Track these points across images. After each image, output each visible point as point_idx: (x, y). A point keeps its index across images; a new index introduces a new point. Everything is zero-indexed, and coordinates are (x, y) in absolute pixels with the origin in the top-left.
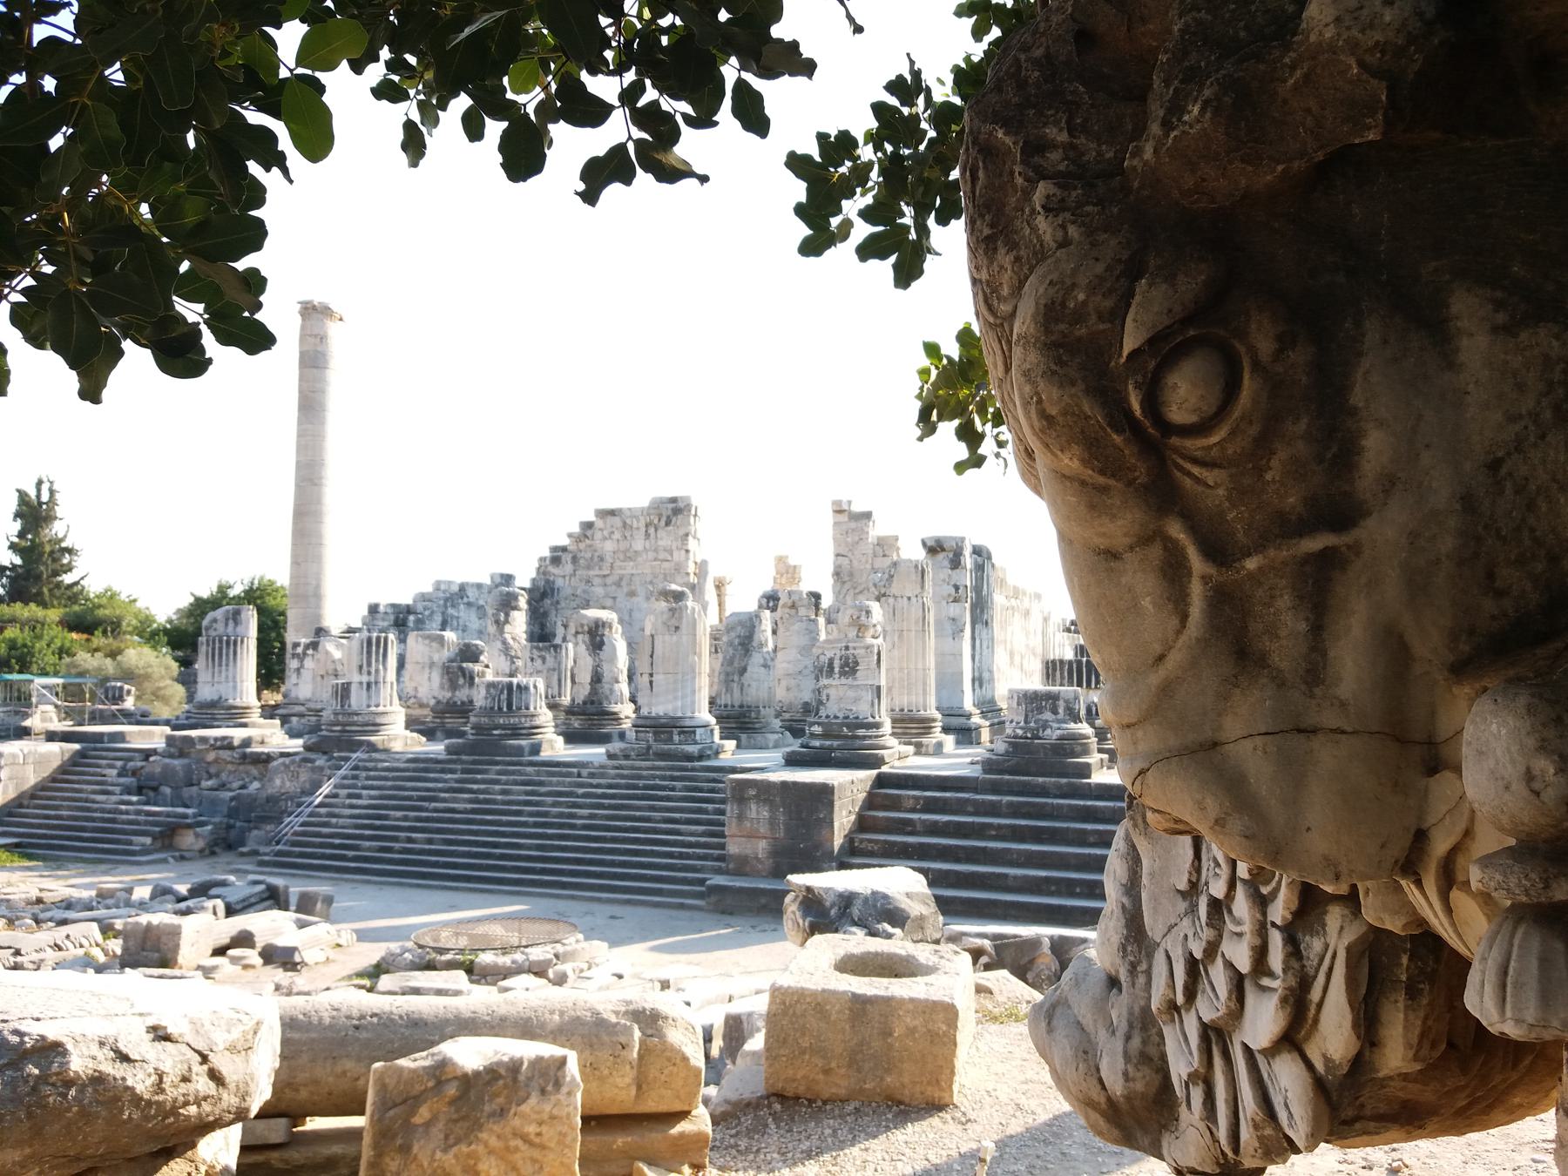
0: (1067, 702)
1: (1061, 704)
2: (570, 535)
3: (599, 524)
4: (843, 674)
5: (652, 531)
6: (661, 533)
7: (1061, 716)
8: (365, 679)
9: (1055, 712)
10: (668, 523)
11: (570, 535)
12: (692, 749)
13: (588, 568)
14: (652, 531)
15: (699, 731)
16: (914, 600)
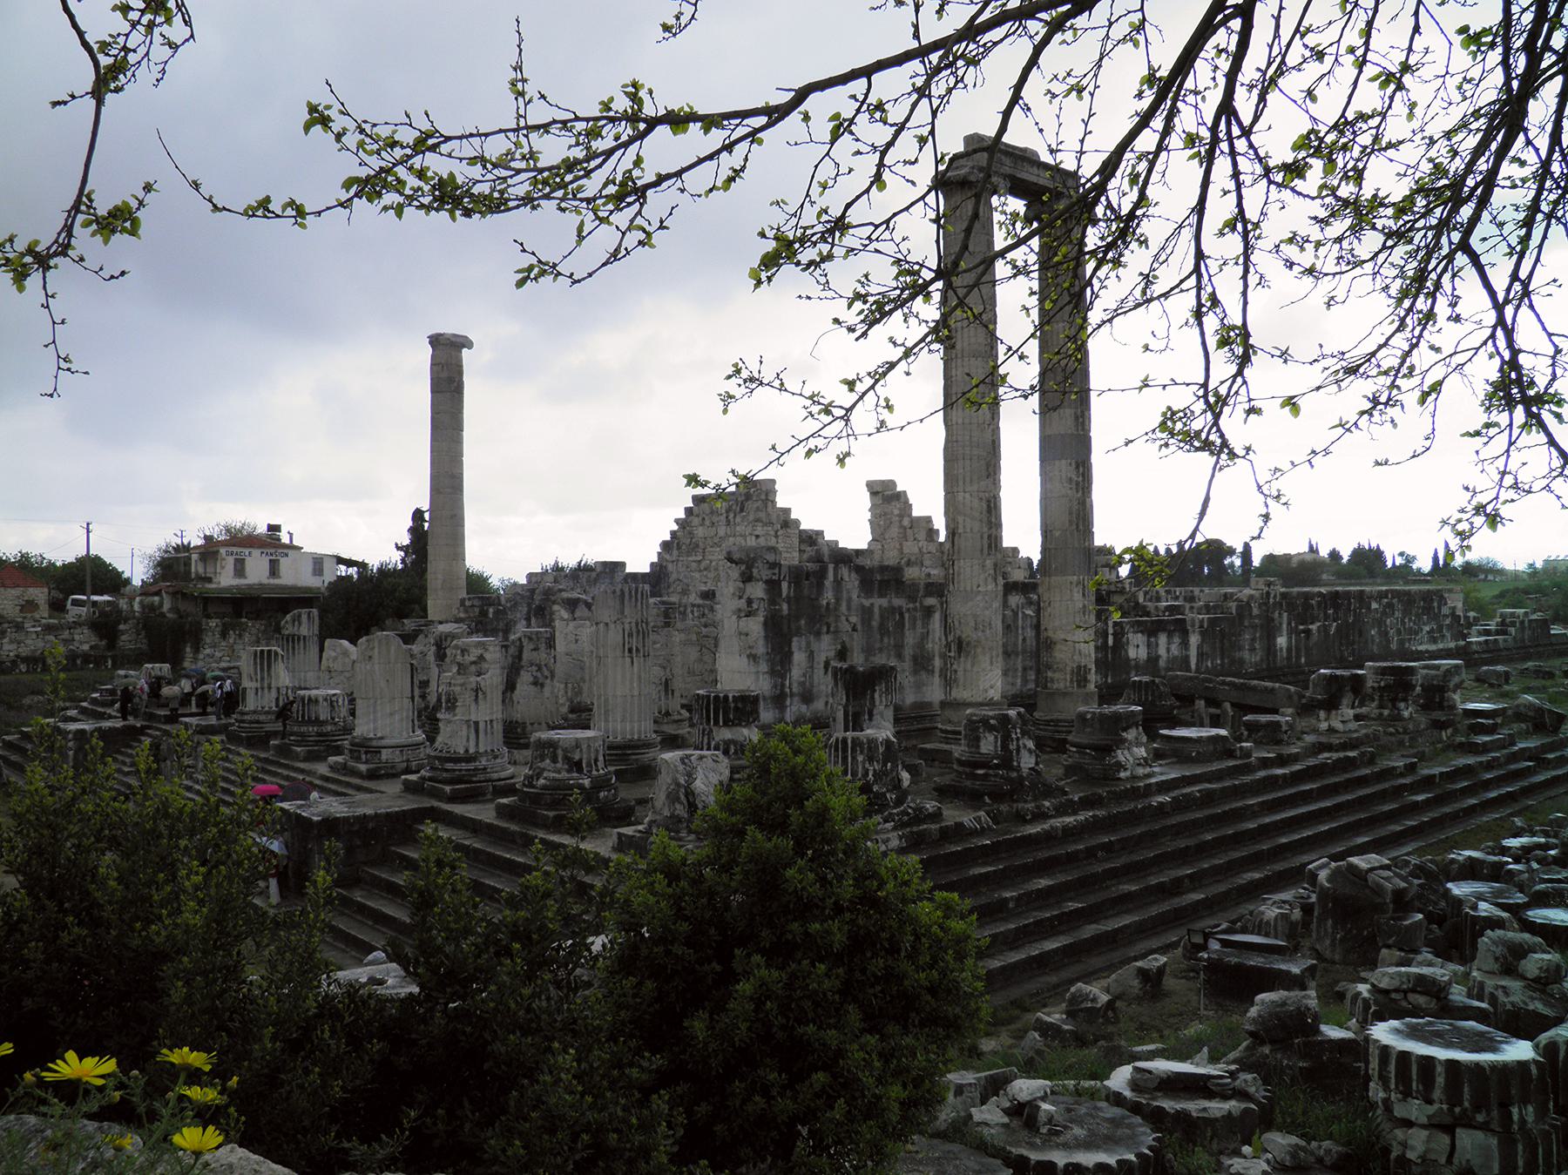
0: (565, 750)
1: (560, 752)
2: (677, 521)
3: (696, 510)
4: (448, 709)
5: (731, 515)
6: (738, 519)
7: (559, 765)
8: (254, 685)
9: (554, 760)
10: (742, 510)
11: (677, 521)
12: (363, 768)
13: (689, 554)
14: (731, 515)
15: (384, 751)
16: (612, 626)
